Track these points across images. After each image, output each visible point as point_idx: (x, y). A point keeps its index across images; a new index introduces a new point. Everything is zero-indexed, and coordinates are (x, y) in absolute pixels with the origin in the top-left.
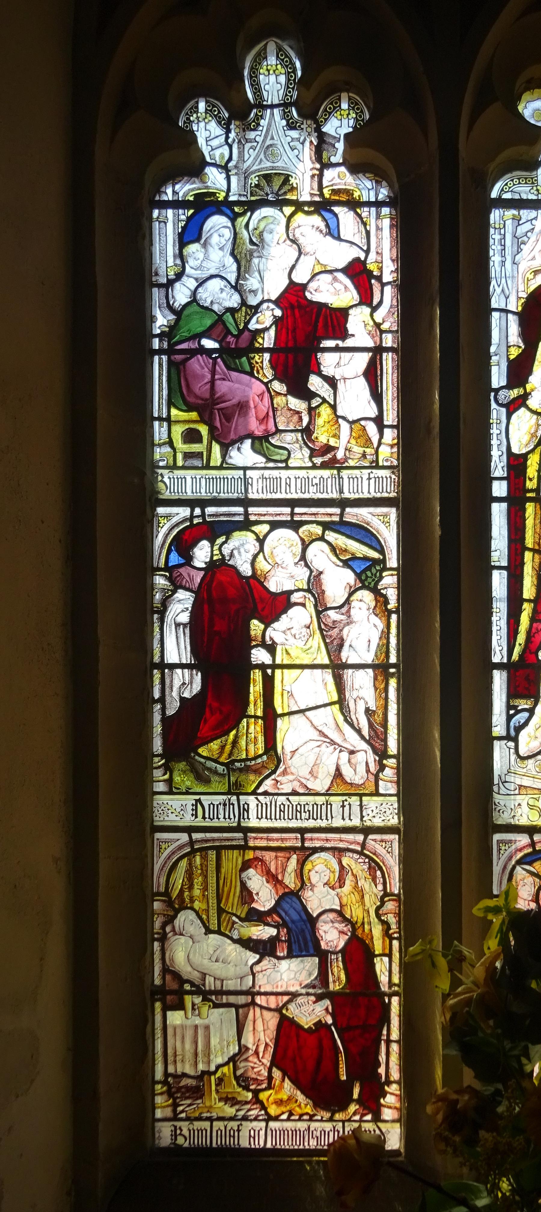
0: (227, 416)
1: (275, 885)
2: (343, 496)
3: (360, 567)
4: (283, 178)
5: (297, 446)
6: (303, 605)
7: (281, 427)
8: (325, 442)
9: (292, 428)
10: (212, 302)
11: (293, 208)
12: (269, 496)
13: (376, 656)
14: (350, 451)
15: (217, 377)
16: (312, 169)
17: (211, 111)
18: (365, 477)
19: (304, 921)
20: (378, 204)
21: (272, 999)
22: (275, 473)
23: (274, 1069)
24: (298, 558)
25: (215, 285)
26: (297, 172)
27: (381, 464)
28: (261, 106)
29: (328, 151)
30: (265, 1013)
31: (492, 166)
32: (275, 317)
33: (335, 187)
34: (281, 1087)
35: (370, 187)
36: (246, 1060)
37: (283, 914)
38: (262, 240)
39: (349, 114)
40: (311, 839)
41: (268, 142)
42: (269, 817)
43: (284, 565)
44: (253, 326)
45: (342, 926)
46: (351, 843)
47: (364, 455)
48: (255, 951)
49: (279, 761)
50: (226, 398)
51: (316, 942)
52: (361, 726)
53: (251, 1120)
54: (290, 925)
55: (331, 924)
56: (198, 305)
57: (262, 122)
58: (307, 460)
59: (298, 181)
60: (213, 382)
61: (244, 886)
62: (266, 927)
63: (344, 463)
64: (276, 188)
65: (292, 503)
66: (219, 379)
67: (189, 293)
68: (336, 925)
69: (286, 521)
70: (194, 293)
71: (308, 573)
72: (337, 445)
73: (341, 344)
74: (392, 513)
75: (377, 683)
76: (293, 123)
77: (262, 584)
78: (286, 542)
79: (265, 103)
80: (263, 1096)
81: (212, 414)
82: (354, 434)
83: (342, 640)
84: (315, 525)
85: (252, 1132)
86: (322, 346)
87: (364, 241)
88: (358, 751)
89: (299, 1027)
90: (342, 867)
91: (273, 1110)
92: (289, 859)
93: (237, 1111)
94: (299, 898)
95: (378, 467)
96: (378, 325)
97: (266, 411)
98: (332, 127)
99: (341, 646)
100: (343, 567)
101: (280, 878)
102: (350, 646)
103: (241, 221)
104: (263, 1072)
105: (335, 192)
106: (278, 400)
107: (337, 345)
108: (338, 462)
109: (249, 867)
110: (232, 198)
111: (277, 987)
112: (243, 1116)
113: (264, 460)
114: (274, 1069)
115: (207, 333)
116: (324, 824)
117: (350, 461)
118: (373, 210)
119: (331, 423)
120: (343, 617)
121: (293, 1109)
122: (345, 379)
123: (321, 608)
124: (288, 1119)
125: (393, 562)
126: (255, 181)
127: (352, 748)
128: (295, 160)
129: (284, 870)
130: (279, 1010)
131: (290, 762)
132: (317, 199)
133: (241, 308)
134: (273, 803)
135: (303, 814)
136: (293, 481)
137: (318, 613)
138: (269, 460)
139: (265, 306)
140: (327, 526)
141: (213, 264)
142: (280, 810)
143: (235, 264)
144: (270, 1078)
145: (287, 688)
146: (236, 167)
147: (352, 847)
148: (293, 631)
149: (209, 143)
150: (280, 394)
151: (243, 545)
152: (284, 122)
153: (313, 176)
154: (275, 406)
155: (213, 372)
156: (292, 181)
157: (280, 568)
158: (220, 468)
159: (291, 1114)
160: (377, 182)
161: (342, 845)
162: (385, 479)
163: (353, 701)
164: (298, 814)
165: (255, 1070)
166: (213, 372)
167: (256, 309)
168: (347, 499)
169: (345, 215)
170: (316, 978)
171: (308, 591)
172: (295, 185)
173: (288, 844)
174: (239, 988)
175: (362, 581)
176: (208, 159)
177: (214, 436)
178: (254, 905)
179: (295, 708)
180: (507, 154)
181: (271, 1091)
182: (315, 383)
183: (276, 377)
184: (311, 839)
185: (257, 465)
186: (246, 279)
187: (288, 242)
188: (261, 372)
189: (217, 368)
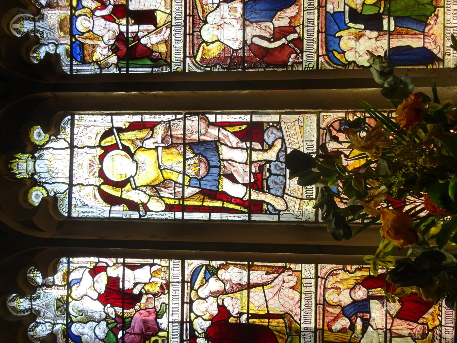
0: (148, 328)
1: (339, 318)
2: (180, 281)
3: (208, 275)
4: (58, 301)
5: (160, 299)
6: (223, 300)
7: (153, 306)
8: (159, 288)
9: (153, 301)
10: (104, 333)
11: (69, 297)
12: (180, 312)
13: (244, 270)
14: (163, 278)
15: (133, 332)
16: (55, 289)
17: (33, 330)
18: (173, 272)
19: (354, 306)
20: (69, 263)
21: (388, 321)
22: (171, 309)
23: (419, 322)
24: (204, 301)
25: (98, 332)
26: (55, 296)
27: (168, 265)
28: (31, 309)
29: (48, 282)
30: (394, 324)
31: (56, 218)
32: (110, 307)
33: (62, 280)
34: (427, 319)
35: (62, 266)
36: (415, 334)
37: (351, 314)
38: (81, 311)
39: (35, 273)
40: (320, 301)
41: (45, 307)
42: (310, 319)
43: (207, 307)
44: (113, 316)
45: (357, 289)
46: (322, 283)
47: (165, 272)
48: (367, 327)
49: (287, 313)
50: (141, 328)
51: (363, 300)
52: (273, 277)
53: (441, 333)
54: (356, 312)
55: (356, 294)
56: (105, 338)
57: (37, 309)
58: (166, 296)
59: (59, 295)
60: (135, 334)
61: (340, 331)
62: (357, 322)
63: (167, 280)
64: (62, 304)
65: (183, 303)
66: (134, 331)
67: (100, 342)
68: (356, 291)
69: (190, 305)
70: (100, 340)
71: (210, 297)
72: (160, 283)
73: (121, 280)
74: (187, 261)
75: (255, 270)
76: (38, 297)
77: (214, 317)
78: (198, 306)
79: (30, 307)
80: (431, 327)
81: (147, 335)
82: (156, 276)
83: (237, 284)
84: (191, 294)
85: (446, 333)
86: (122, 288)
87: (82, 269)
88: (283, 279)
89: (400, 310)
90: (332, 288)
91: (437, 323)
92: (328, 311)
93: (437, 339)
94: (345, 307)
95: (169, 266)
96: (114, 264)
97: (146, 312)
98: (39, 280)
99: (240, 284)
100: (208, 282)
101: (336, 315)
102: (240, 280)
103: (74, 319)
104: (420, 327)
105: (64, 280)
106: (142, 307)
107: (121, 281)
108: (167, 283)
109: (331, 329)
110: (65, 323)
111: (383, 319)
112: (439, 336)
113: (165, 314)
114: (419, 322)
115: (116, 335)
116: (313, 296)
117: (166, 278)
118: (71, 265)
119: (152, 285)
120: (228, 283)
121: (437, 314)
122: (135, 279)
123: (225, 292)
124: (441, 316)
125: (207, 262)
126: (59, 313)
127: (282, 281)
128: (51, 296)
129: (333, 313)
130: (393, 319)
131: (288, 309)
132: (66, 287)
133: (107, 321)
134: (304, 316)
135: (309, 304)
136: (174, 302)
137: (227, 293)
138: (165, 312)
139: (106, 311)
140: (192, 289)
141: (90, 331)
142: (307, 314)
143: (90, 322)
144: (423, 324)
145: (257, 308)
146: (53, 320)
147: (323, 283)
148: (234, 304)
149: (44, 331)
150: (140, 306)
151: (199, 324)
152: (37, 300)
153: (58, 289)
154: (144, 308)
155: (131, 334)
156: (59, 297)
157: (208, 309)
158: (168, 332)
159: (439, 315)
160: (60, 263)
161: (322, 288)
162: (174, 263)
163: (263, 280)
164: (309, 306)
165: (419, 330)
166: (131, 334)
167: (107, 315)
168: (182, 280)
169: (73, 276)
170: (380, 302)
171: (217, 297)
172: (61, 296)
173: (322, 311)
174: (384, 336)
175: (214, 275)
176: (50, 332)
177: (156, 335)
178: (347, 327)
179: (265, 305)
180: (51, 212)
181: (429, 324)
182: (136, 291)
183: (134, 307)
184: (320, 301)
185: (167, 317)
186: (96, 318)
187: (82, 300)
188: (131, 314)
189: (129, 332)
